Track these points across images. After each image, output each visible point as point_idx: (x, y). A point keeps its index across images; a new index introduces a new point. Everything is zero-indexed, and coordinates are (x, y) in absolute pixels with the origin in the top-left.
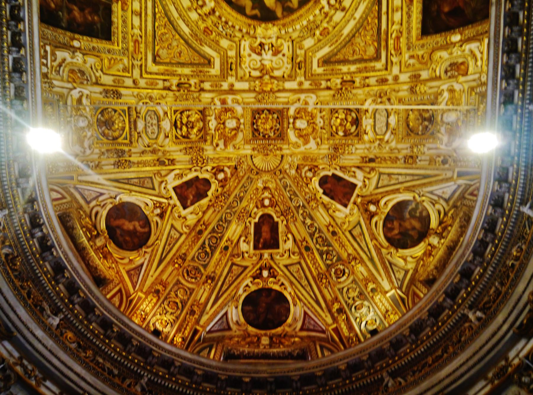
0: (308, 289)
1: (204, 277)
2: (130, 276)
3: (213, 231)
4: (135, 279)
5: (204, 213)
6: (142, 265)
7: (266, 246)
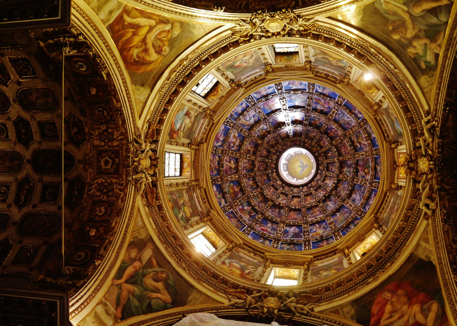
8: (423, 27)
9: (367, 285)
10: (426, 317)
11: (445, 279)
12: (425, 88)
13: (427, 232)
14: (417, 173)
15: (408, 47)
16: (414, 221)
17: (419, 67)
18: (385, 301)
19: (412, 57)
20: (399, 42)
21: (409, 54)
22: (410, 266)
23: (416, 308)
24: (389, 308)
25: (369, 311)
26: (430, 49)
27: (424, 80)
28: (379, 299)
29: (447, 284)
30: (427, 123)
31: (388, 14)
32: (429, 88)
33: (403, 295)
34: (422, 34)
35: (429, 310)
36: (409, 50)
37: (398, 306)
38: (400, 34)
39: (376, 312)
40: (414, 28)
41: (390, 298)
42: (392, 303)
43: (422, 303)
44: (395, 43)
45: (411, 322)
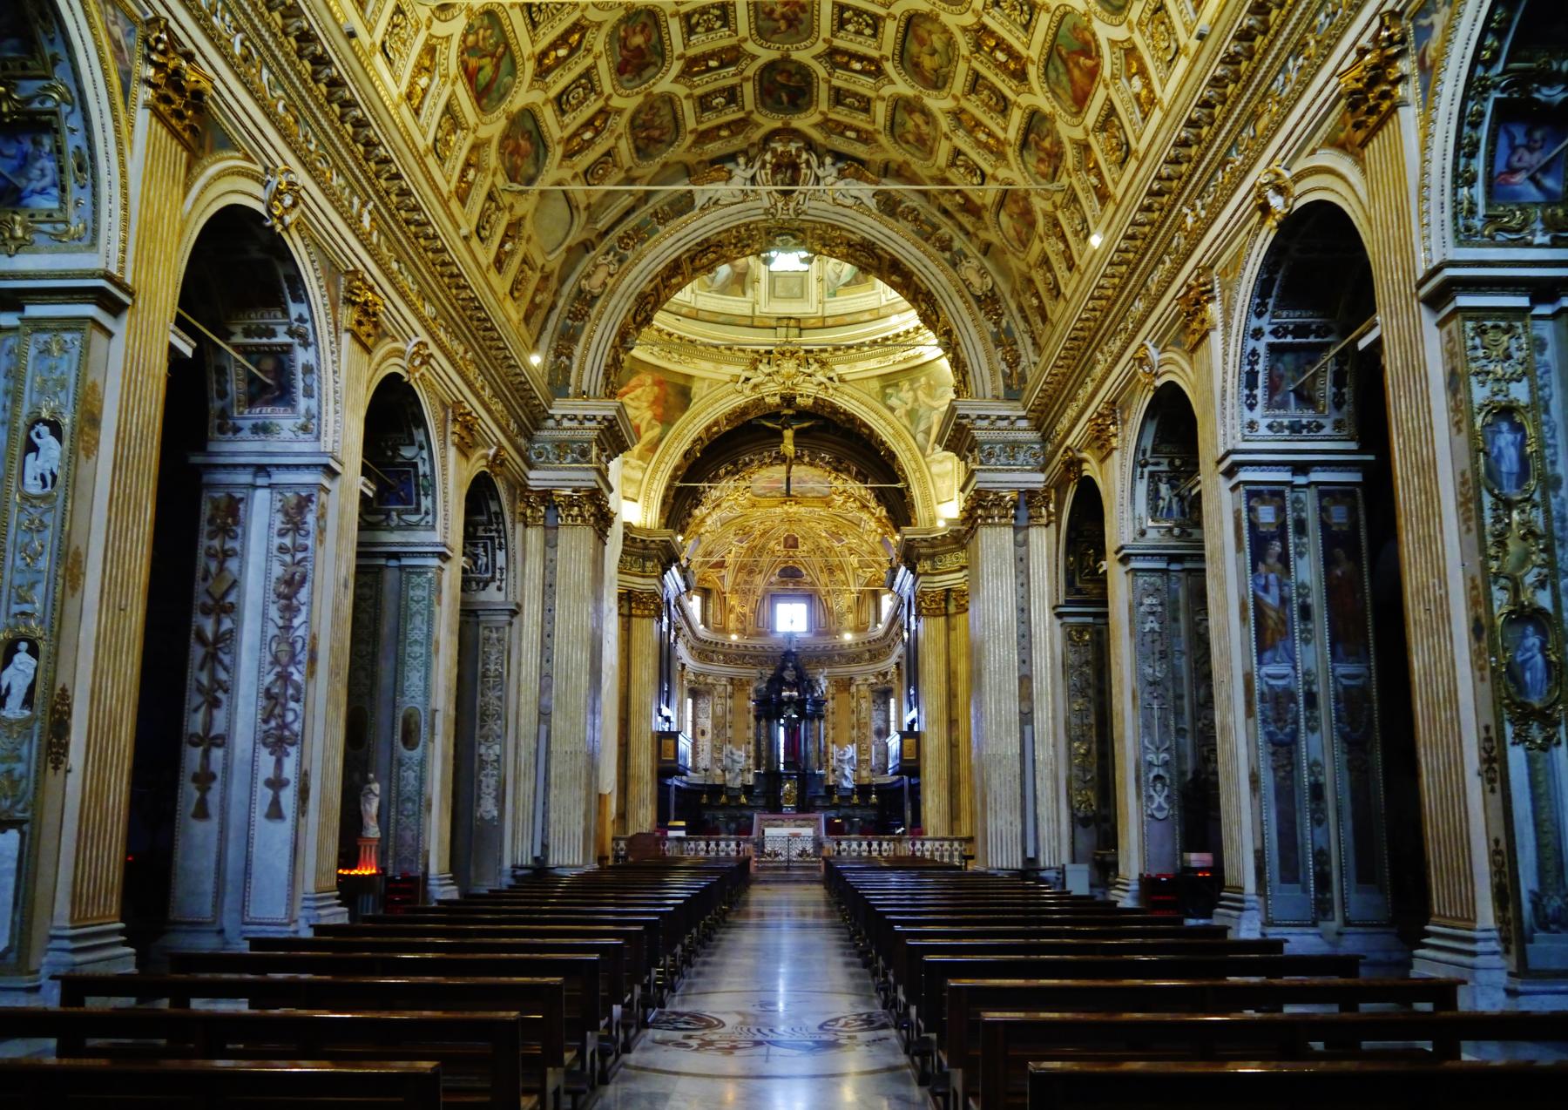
8: (921, 411)
20: (918, 379)
22: (681, 382)
23: (648, 415)
24: (639, 391)
27: (875, 385)
28: (642, 376)
30: (831, 379)
43: (655, 417)
45: (637, 421)
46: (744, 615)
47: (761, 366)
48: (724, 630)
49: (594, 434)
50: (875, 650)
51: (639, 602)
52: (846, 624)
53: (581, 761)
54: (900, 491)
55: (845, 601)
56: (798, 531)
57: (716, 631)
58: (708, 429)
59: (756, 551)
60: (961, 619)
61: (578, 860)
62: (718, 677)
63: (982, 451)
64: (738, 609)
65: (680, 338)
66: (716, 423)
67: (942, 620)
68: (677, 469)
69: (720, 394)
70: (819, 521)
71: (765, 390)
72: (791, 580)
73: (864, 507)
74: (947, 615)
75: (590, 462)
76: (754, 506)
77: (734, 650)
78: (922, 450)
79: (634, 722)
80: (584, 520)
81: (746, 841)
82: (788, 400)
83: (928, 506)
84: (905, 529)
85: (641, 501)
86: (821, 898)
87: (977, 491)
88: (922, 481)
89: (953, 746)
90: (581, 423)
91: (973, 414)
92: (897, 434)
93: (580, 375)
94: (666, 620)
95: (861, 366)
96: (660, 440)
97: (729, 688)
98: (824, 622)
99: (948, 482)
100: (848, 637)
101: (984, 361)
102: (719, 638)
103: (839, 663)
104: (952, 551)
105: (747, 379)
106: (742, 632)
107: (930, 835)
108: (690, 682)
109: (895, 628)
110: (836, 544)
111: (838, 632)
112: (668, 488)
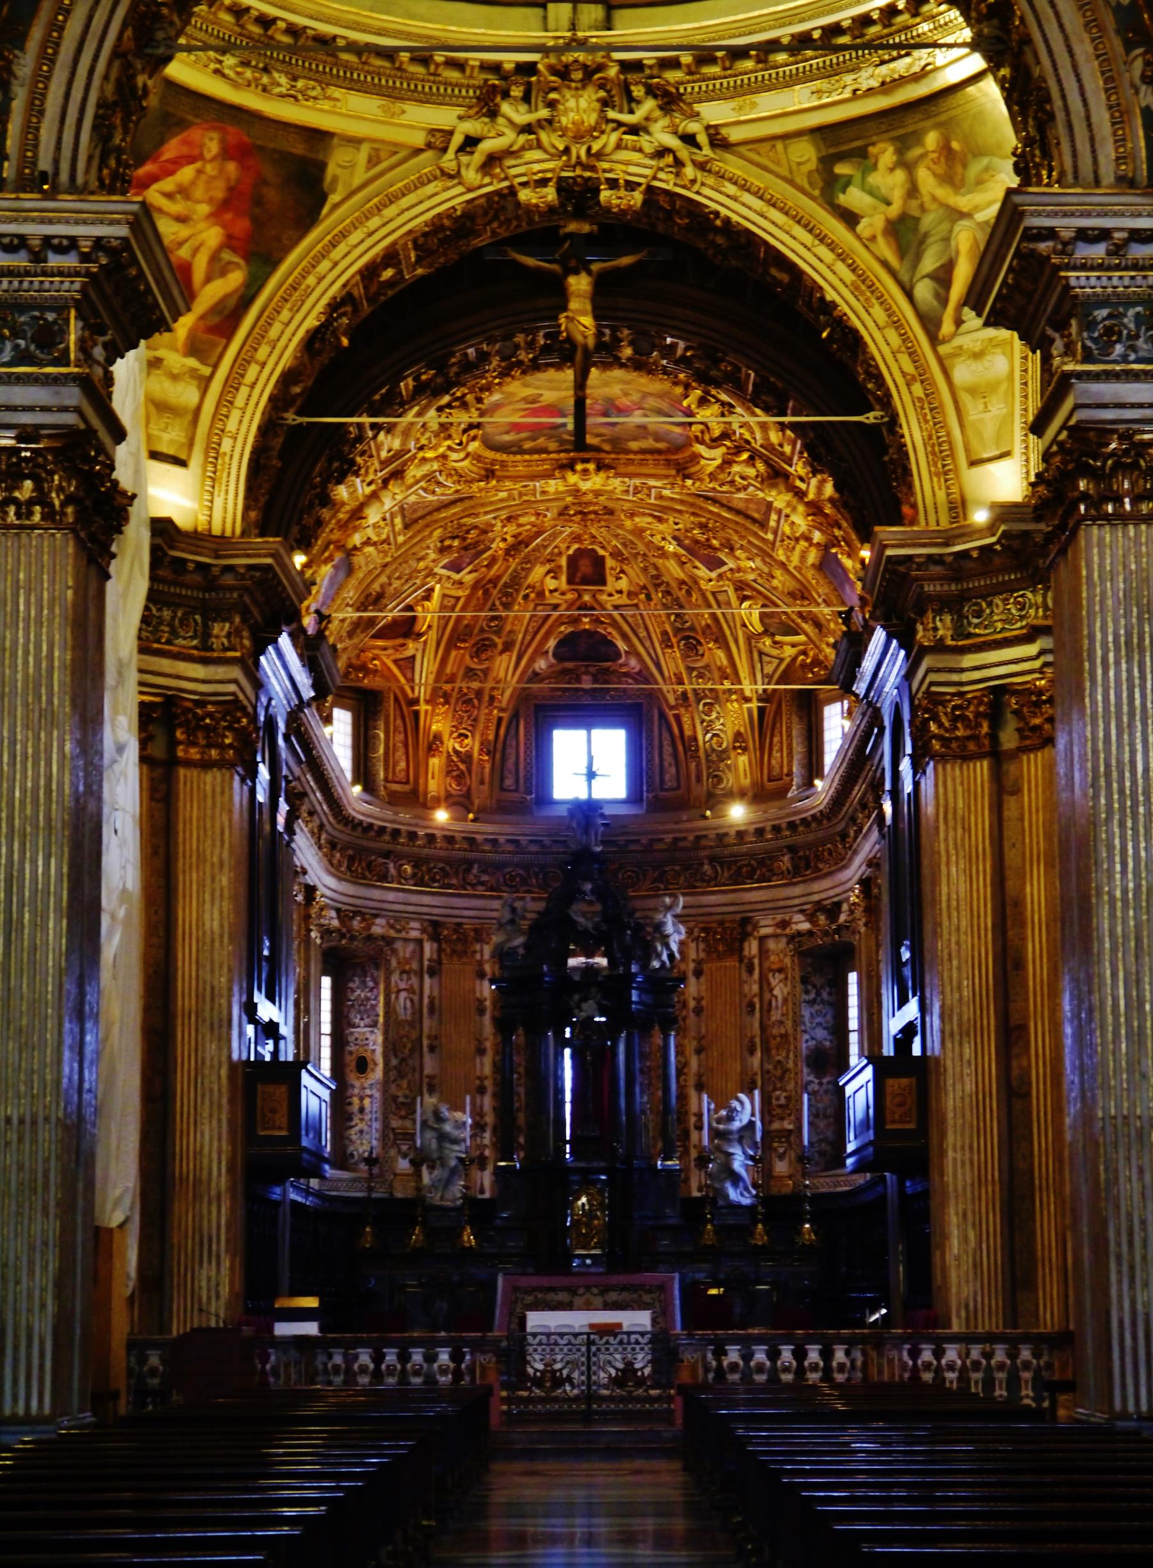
0: (648, 644)
1: (500, 647)
2: (399, 667)
3: (506, 585)
4: (409, 675)
5: (489, 566)
6: (413, 657)
7: (586, 581)
8: (927, 222)
9: (216, 71)
10: (208, 279)
11: (304, 278)
12: (786, 148)
13: (396, 153)
14: (554, 89)
15: (900, 152)
16: (416, 90)
17: (841, 157)
18: (196, 152)
19: (873, 150)
21: (881, 146)
22: (299, 149)
23: (213, 236)
24: (186, 173)
25: (162, 142)
26: (875, 208)
27: (806, 154)
28: (195, 134)
29: (295, 289)
30: (689, 139)
31: (987, 169)
32: (784, 162)
33: (228, 180)
34: (913, 208)
35: (223, 273)
36: (891, 149)
37: (199, 192)
38: (935, 155)
39: (164, 158)
40: (934, 199)
41: (208, 156)
42: (199, 172)
43: (230, 242)
44: (921, 125)
45: (184, 253)
46: (466, 758)
47: (506, 108)
48: (415, 799)
49: (72, 287)
50: (807, 848)
51: (194, 727)
52: (729, 781)
53: (48, 1136)
54: (874, 427)
55: (731, 719)
56: (603, 539)
57: (394, 800)
58: (370, 272)
59: (495, 592)
60: (1032, 766)
61: (40, 1402)
62: (398, 920)
63: (1089, 325)
64: (451, 744)
65: (293, 30)
66: (390, 257)
67: (982, 769)
68: (288, 378)
69: (398, 177)
70: (660, 513)
71: (517, 170)
72: (588, 677)
73: (776, 476)
74: (998, 757)
75: (63, 361)
76: (489, 474)
77: (440, 850)
78: (930, 324)
79: (184, 1038)
80: (50, 515)
81: (478, 1346)
82: (578, 194)
83: (945, 472)
84: (885, 532)
85: (196, 460)
86: (676, 1495)
87: (1077, 431)
88: (930, 406)
89: (1013, 1092)
90: (37, 257)
91: (1066, 225)
92: (864, 284)
93: (31, 130)
94: (264, 772)
95: (769, 103)
96: (244, 300)
97: (428, 949)
98: (669, 772)
99: (997, 408)
100: (737, 813)
101: (1094, 83)
102: (404, 817)
103: (714, 880)
104: (1007, 589)
105: (471, 142)
106: (460, 803)
107: (956, 1327)
108: (326, 932)
109: (857, 792)
110: (703, 572)
111: (716, 800)
112: (267, 429)
